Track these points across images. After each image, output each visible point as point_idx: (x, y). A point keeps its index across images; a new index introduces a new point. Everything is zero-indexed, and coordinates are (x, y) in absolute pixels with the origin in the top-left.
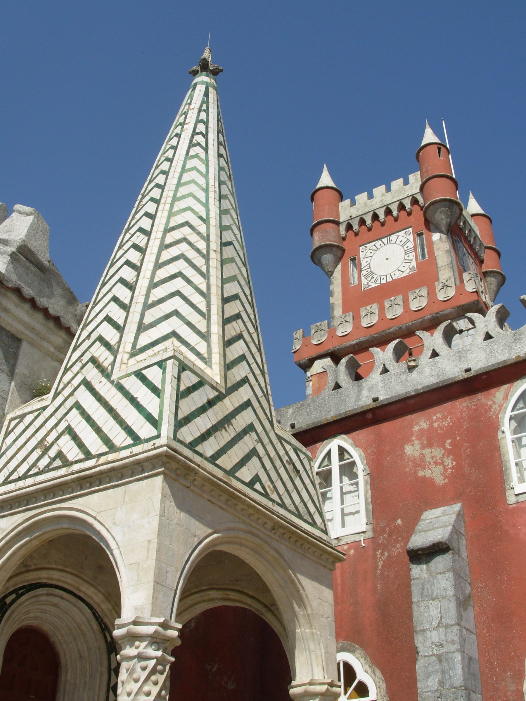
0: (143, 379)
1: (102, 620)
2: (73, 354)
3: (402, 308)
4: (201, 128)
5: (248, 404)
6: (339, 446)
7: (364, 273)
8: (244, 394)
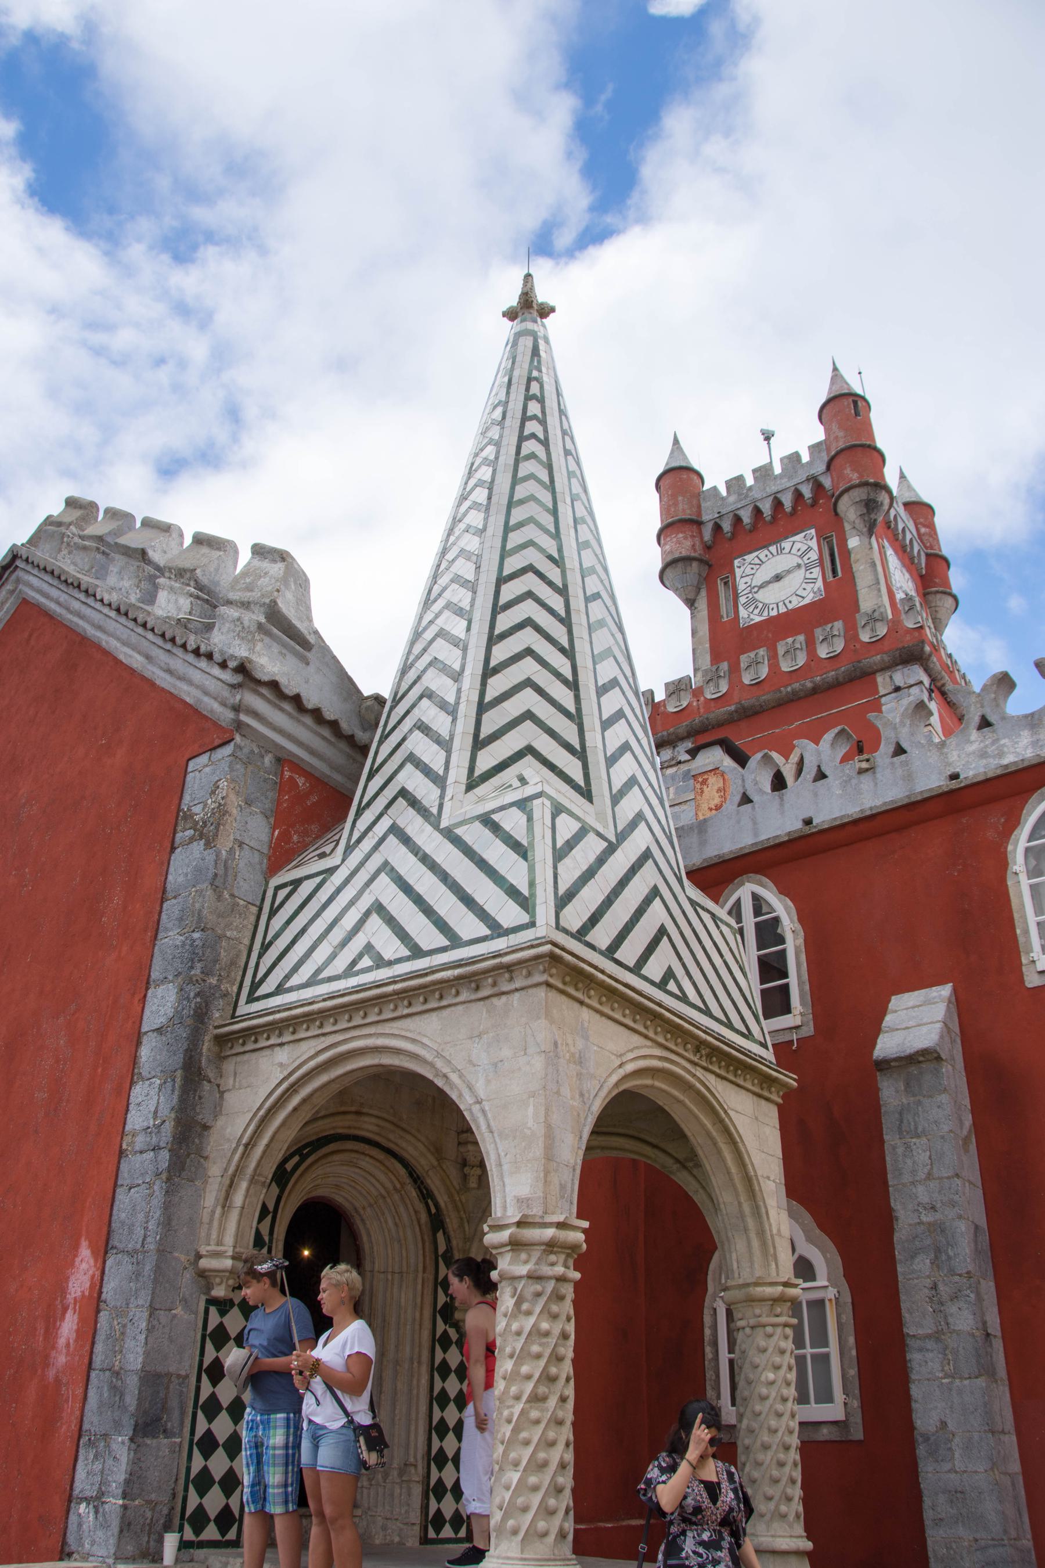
0: (495, 828)
1: (422, 1183)
2: (370, 784)
3: (805, 653)
4: (534, 408)
6: (753, 893)
7: (742, 600)
8: (640, 840)
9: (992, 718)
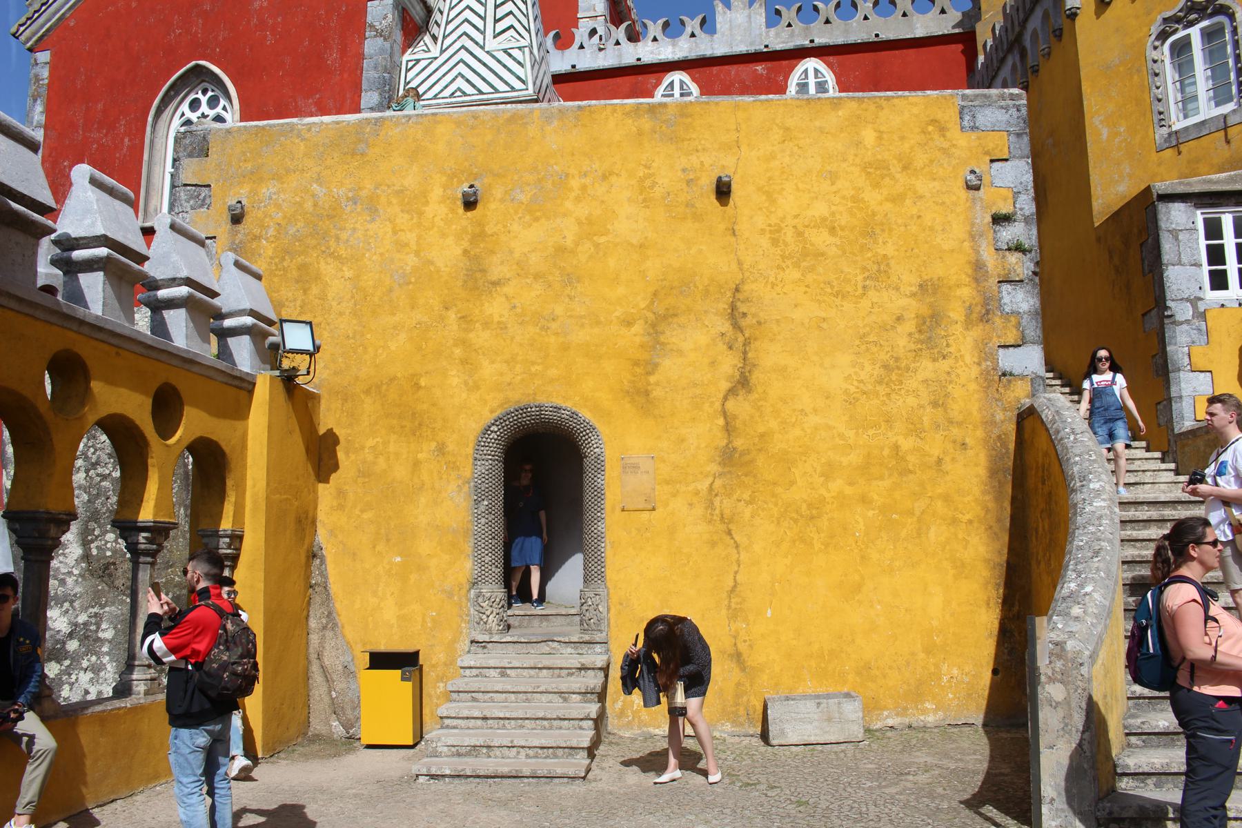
0: (510, 55)
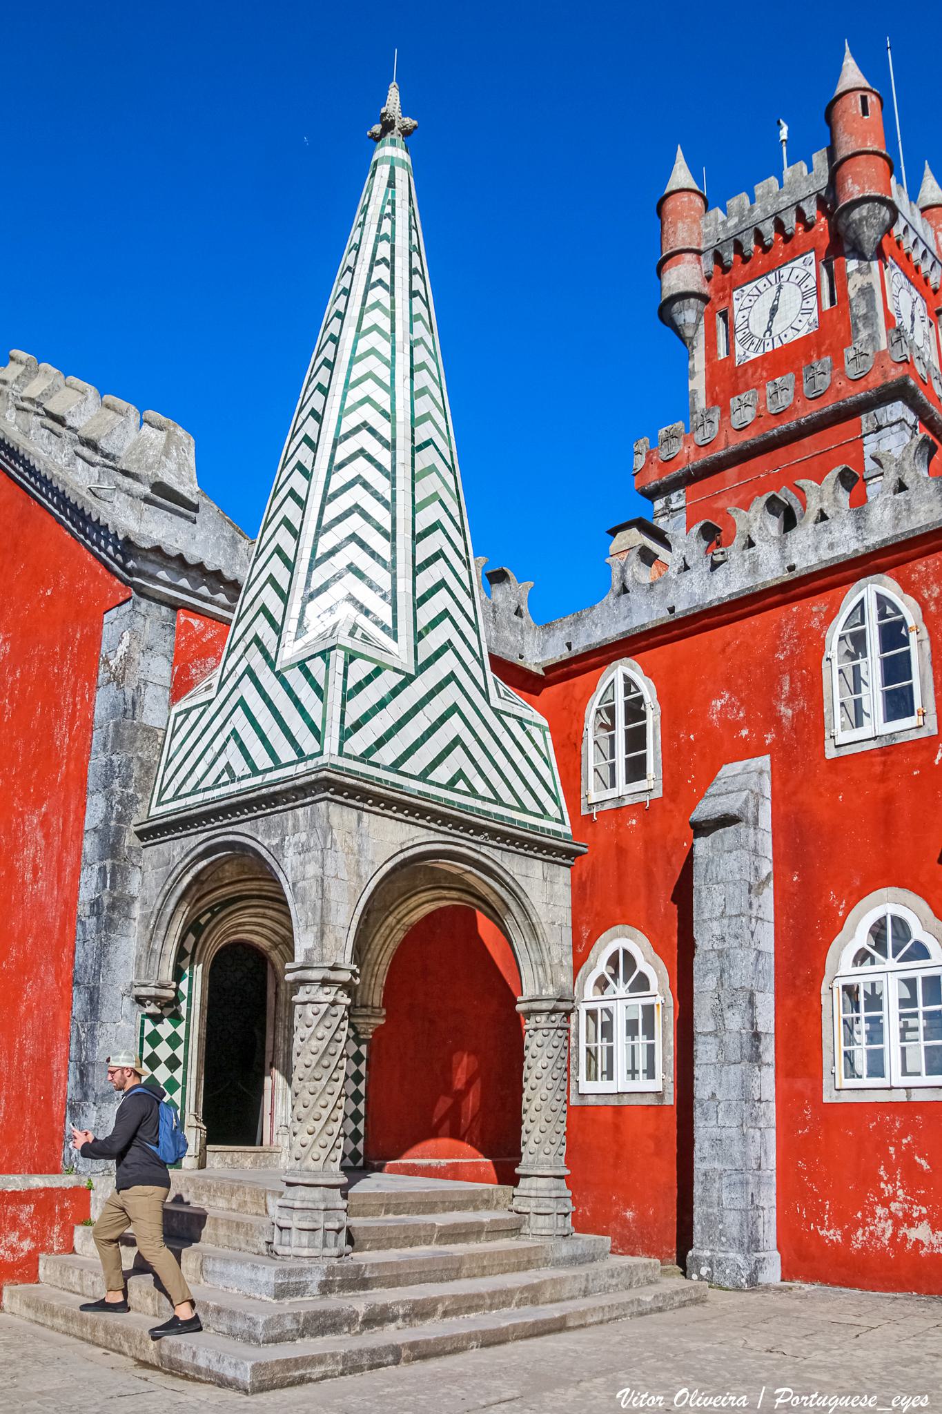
0: (307, 674)
5: (452, 677)
8: (447, 663)
9: (828, 513)
